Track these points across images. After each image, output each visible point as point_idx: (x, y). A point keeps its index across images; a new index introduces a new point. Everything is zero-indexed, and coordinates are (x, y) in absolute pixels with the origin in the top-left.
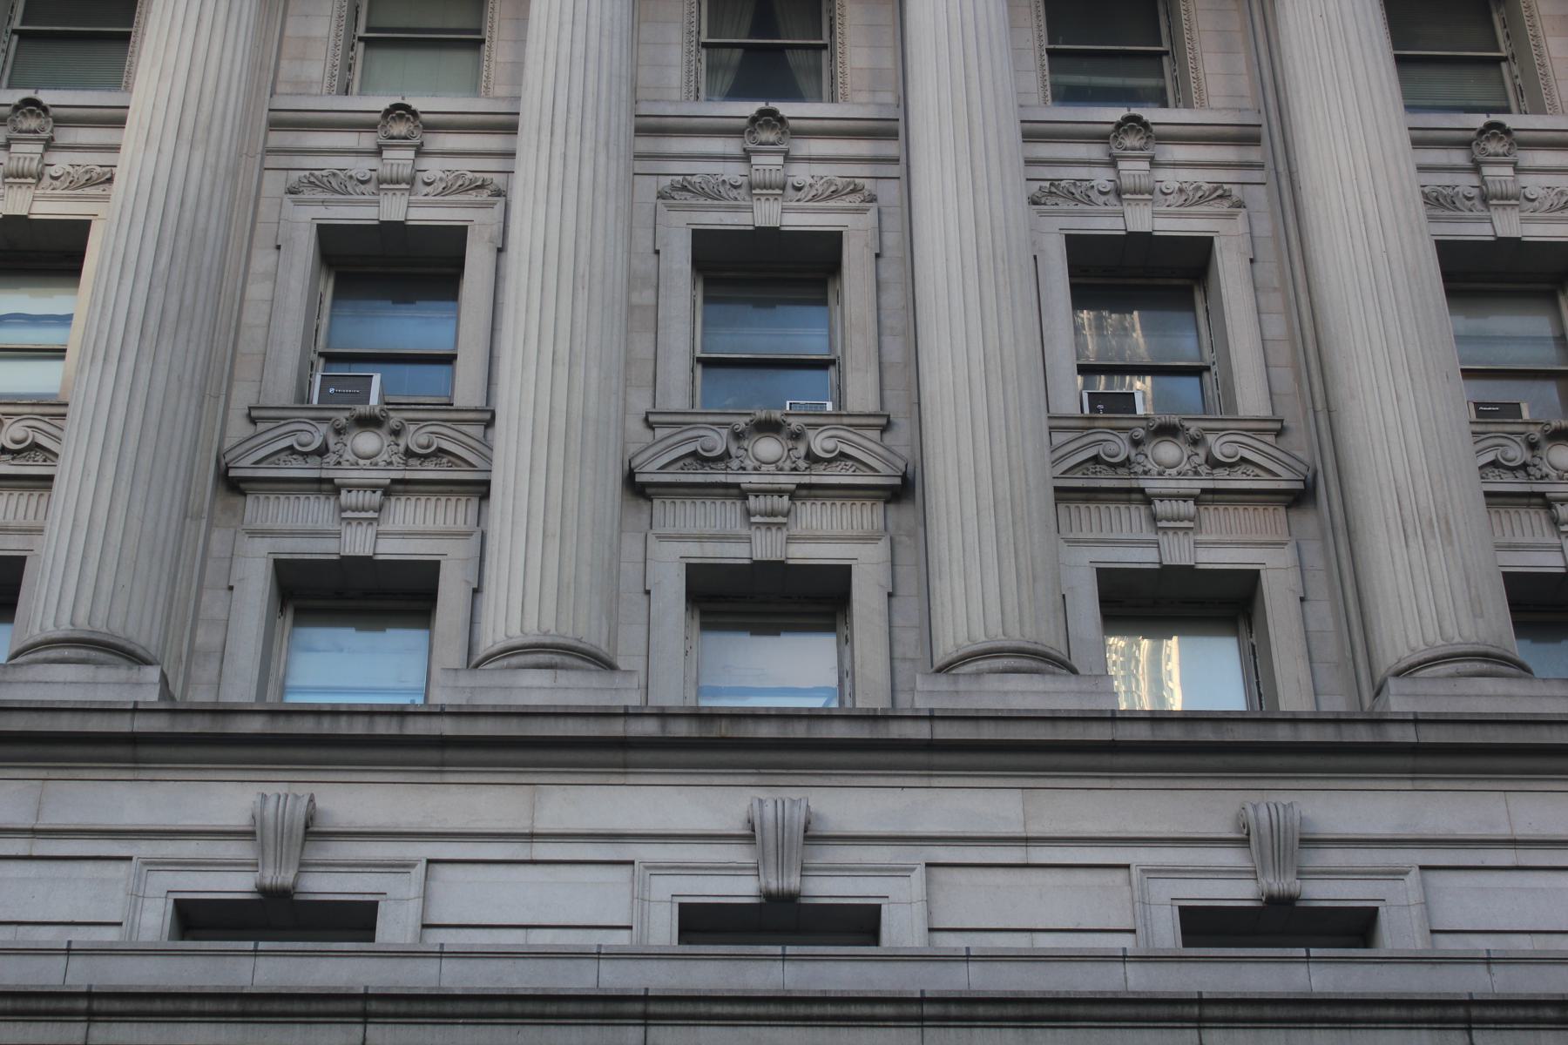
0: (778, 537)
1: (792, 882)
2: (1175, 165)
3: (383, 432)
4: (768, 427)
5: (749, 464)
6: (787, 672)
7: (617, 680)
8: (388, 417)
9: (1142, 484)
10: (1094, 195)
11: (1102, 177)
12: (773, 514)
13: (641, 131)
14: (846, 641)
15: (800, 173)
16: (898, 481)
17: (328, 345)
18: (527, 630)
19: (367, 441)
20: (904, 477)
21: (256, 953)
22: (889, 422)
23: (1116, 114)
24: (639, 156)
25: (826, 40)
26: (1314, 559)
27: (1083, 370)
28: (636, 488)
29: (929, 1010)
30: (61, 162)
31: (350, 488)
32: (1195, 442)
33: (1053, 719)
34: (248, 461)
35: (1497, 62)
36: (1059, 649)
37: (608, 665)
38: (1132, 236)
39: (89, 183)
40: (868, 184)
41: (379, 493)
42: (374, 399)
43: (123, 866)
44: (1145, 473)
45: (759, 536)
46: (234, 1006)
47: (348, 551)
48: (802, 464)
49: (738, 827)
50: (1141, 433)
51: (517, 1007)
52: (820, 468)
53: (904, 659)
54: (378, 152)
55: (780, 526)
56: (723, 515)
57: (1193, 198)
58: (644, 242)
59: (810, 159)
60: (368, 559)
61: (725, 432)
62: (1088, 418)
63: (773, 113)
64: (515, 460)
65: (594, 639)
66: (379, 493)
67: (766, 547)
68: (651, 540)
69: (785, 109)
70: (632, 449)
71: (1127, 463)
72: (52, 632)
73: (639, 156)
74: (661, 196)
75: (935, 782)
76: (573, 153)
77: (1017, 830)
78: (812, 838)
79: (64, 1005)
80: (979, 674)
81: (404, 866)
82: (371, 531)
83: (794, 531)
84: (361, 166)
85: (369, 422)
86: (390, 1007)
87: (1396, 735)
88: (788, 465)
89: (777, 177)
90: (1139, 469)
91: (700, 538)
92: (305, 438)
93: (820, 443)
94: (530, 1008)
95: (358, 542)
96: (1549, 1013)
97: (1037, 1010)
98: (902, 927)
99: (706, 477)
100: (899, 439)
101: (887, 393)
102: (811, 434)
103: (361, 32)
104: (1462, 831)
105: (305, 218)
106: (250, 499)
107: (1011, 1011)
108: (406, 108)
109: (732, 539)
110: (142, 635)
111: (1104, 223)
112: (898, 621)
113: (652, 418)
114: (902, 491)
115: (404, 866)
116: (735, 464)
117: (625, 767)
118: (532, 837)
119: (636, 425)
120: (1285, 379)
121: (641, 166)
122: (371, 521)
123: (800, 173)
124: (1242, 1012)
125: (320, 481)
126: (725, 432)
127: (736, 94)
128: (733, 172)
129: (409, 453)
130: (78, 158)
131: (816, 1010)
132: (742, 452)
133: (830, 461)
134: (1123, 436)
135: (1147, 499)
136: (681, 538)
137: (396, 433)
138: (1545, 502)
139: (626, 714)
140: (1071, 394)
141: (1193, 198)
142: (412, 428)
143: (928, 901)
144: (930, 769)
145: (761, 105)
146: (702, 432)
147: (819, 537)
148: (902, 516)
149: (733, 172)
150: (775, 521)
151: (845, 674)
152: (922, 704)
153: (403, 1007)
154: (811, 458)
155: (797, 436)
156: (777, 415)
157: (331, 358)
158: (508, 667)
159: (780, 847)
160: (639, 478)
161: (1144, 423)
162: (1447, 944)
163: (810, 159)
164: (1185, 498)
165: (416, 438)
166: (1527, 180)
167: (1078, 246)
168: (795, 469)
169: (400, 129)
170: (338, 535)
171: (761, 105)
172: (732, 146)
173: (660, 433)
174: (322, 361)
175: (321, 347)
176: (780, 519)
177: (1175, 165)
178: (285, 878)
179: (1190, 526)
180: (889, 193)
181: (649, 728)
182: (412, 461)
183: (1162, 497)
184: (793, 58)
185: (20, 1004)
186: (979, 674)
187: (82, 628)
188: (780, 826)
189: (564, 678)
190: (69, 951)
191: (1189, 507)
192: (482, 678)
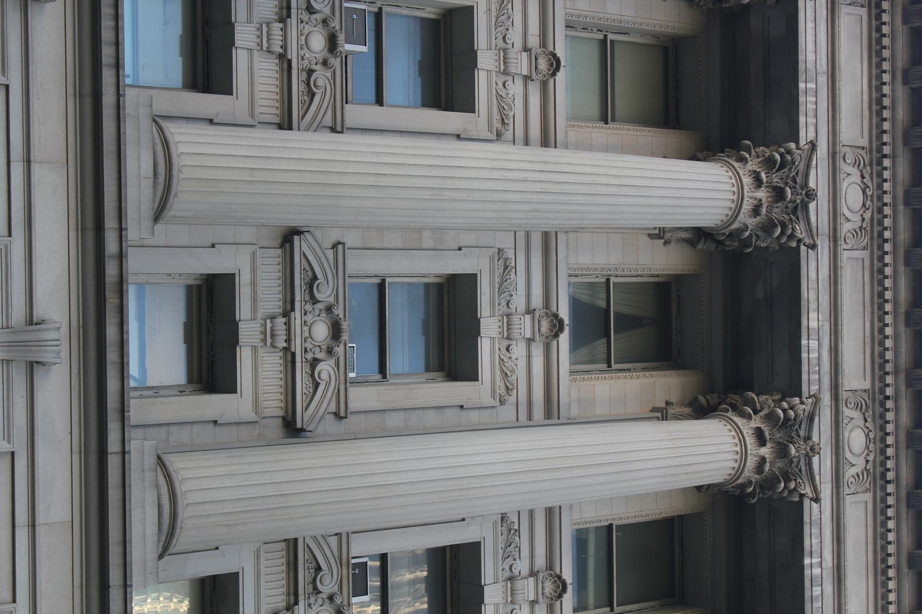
0: (256, 340)
3: (325, 54)
4: (336, 331)
5: (309, 318)
6: (156, 349)
7: (147, 223)
8: (336, 57)
9: (301, 603)
10: (510, 561)
11: (522, 566)
12: (273, 336)
13: (546, 236)
14: (181, 391)
15: (519, 350)
16: (299, 425)
17: (387, 14)
18: (183, 157)
19: (318, 42)
20: (302, 430)
22: (342, 418)
23: (568, 575)
24: (528, 235)
25: (614, 366)
28: (289, 237)
31: (284, 30)
33: (125, 542)
36: (176, 546)
37: (157, 216)
38: (481, 589)
40: (512, 399)
41: (281, 51)
42: (349, 47)
44: (310, 605)
45: (257, 326)
47: (238, 29)
48: (310, 356)
49: (38, 313)
50: (338, 601)
52: (307, 368)
53: (168, 433)
54: (526, 49)
55: (264, 341)
56: (271, 301)
58: (467, 239)
59: (529, 357)
60: (233, 43)
61: (332, 300)
62: (348, 563)
63: (561, 329)
64: (307, 147)
65: (179, 205)
66: (281, 51)
67: (249, 331)
68: (249, 249)
69: (564, 338)
70: (318, 233)
71: (316, 591)
73: (528, 235)
74: (500, 251)
75: (76, 457)
76: (529, 187)
77: (40, 518)
78: (32, 366)
80: (157, 486)
82: (253, 45)
83: (261, 351)
84: (515, 37)
85: (332, 43)
88: (308, 345)
89: (516, 333)
90: (312, 600)
91: (254, 283)
93: (325, 369)
99: (298, 286)
100: (330, 424)
101: (363, 416)
102: (332, 362)
103: (610, 37)
108: (558, 68)
109: (254, 307)
111: (489, 569)
112: (196, 428)
113: (340, 247)
114: (292, 429)
116: (308, 307)
118: (28, 161)
119: (334, 235)
121: (521, 236)
122: (260, 45)
123: (519, 350)
125: (289, 8)
126: (332, 300)
127: (576, 305)
128: (519, 302)
129: (310, 72)
132: (317, 312)
133: (312, 375)
134: (336, 588)
136: (254, 270)
137: (325, 63)
139: (121, 230)
140: (364, 549)
142: (329, 75)
145: (567, 321)
146: (331, 283)
147: (257, 368)
148: (275, 428)
149: (519, 302)
150: (268, 337)
151: (157, 391)
152: (134, 446)
154: (315, 362)
155: (330, 352)
156: (345, 337)
157: (378, 16)
158: (154, 144)
159: (24, 343)
160: (296, 238)
161: (345, 603)
163: (529, 357)
165: (321, 77)
167: (473, 549)
168: (306, 351)
169: (543, 64)
170: (250, 21)
171: (567, 321)
172: (537, 301)
173: (330, 253)
174: (376, 10)
175: (385, 9)
176: (269, 341)
180: (507, 414)
181: (111, 247)
182: (305, 74)
184: (601, 343)
186: (157, 486)
188: (40, 344)
189: (147, 184)
192: (146, 125)
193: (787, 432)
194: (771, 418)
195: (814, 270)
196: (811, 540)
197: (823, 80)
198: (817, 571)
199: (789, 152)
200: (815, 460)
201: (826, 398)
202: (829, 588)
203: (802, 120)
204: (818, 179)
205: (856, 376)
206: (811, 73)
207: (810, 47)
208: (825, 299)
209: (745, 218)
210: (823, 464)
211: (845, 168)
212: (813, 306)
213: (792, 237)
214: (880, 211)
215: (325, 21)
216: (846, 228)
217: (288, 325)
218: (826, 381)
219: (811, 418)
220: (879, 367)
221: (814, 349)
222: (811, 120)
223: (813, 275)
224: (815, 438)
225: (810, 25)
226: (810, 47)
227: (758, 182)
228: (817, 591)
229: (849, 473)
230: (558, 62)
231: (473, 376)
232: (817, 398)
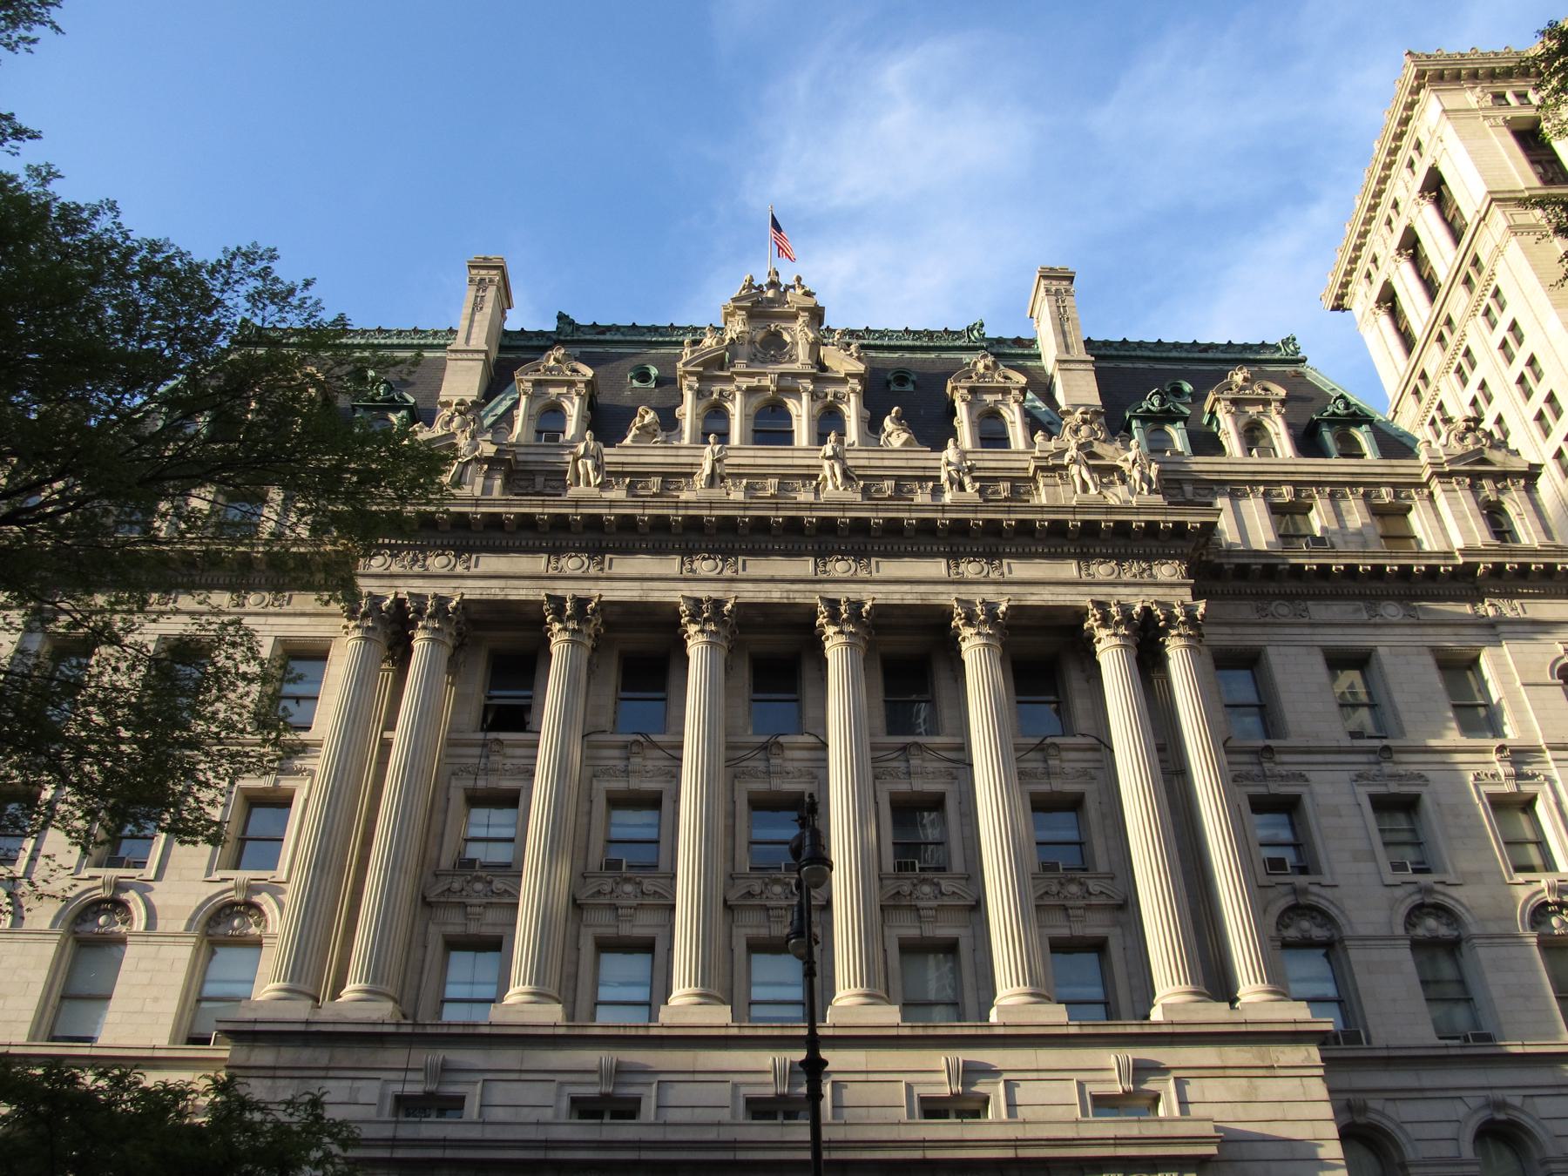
138: (1065, 908)
166: (1065, 765)
178: (610, 1089)
196: (895, 599)
202: (923, 588)
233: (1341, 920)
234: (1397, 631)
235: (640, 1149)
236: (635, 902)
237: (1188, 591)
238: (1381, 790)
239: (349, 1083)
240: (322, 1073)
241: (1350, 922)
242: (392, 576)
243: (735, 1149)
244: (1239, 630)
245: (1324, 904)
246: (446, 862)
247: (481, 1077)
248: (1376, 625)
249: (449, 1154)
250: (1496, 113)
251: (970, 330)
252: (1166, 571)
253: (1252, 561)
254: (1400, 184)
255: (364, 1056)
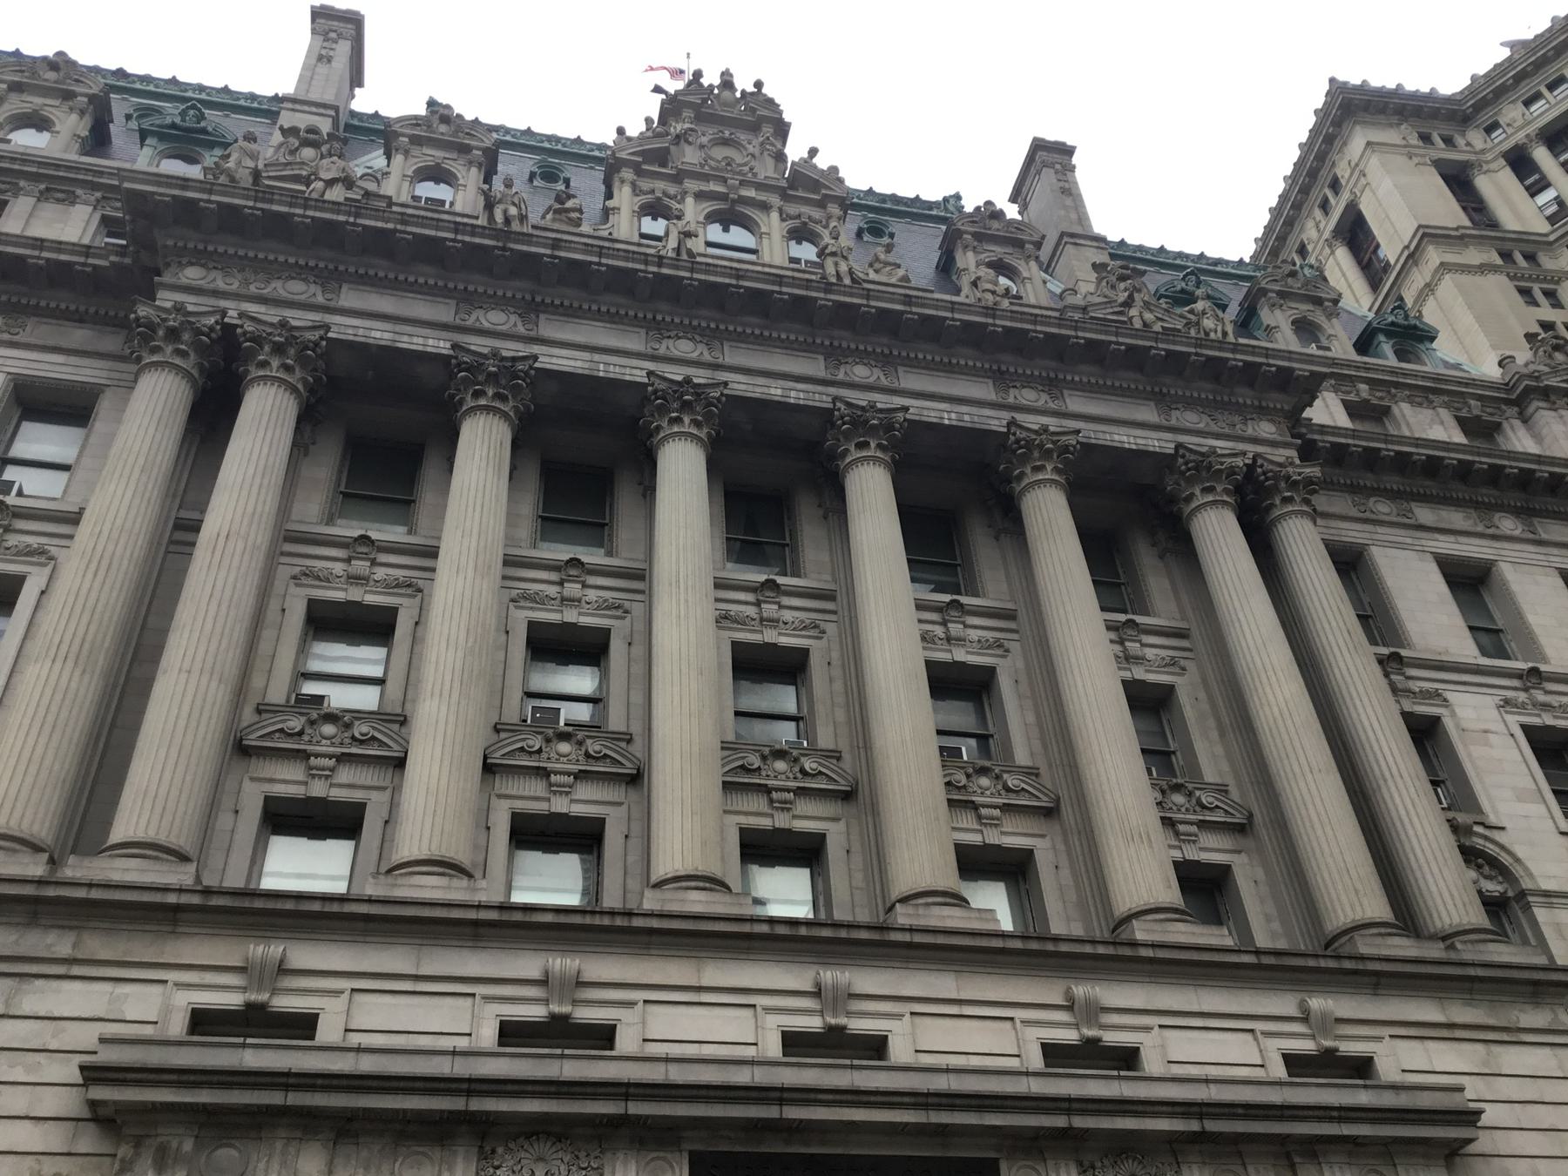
1: (842, 1021)
2: (975, 627)
15: (788, 615)
19: (564, 747)
21: (562, 1056)
26: (1061, 847)
27: (939, 732)
29: (930, 1100)
30: (380, 573)
32: (998, 777)
34: (498, 755)
35: (1119, 585)
39: (397, 586)
40: (822, 624)
43: (469, 1000)
46: (553, 1089)
51: (712, 1093)
52: (809, 779)
55: (788, 810)
57: (984, 645)
63: (774, 581)
67: (782, 821)
72: (416, 854)
79: (454, 1086)
80: (928, 905)
81: (630, 1004)
85: (564, 737)
86: (641, 1091)
87: (1144, 952)
92: (531, 743)
93: (809, 765)
94: (718, 1093)
95: (560, 805)
96: (1240, 1111)
97: (987, 1102)
98: (899, 1051)
102: (803, 759)
104: (1176, 1007)
105: (521, 618)
106: (498, 777)
107: (974, 1102)
108: (578, 560)
110: (463, 856)
111: (941, 656)
115: (630, 1004)
117: (748, 950)
118: (700, 989)
120: (1037, 744)
122: (567, 793)
124: (1090, 1106)
125: (538, 768)
129: (588, 755)
130: (390, 571)
131: (872, 1099)
133: (813, 776)
135: (974, 807)
137: (580, 743)
141: (984, 645)
143: (913, 1034)
144: (907, 959)
150: (785, 807)
153: (648, 1091)
154: (803, 772)
159: (835, 999)
162: (1177, 1070)
164: (995, 807)
165: (593, 747)
169: (573, 572)
177: (975, 627)
179: (994, 823)
181: (765, 928)
183: (984, 806)
185: (428, 1085)
186: (928, 905)
187: (436, 852)
190: (454, 1053)
191: (997, 812)
193: (862, 424)
194: (848, 436)
195: (741, 385)
197: (597, 357)
198: (953, 416)
199: (655, 392)
200: (879, 405)
201: (832, 390)
202: (964, 409)
203: (627, 378)
204: (676, 373)
205: (815, 366)
206: (593, 366)
207: (572, 363)
208: (761, 381)
209: (703, 434)
210: (883, 401)
211: (662, 351)
212: (766, 390)
213: (718, 400)
214: (695, 328)
215: (548, 741)
216: (707, 357)
217: (778, 790)
218: (820, 388)
219: (849, 405)
220: (808, 348)
221: (797, 395)
222: (628, 371)
223: (743, 387)
224: (864, 404)
225: (554, 360)
226: (572, 363)
227: (678, 420)
228: (967, 418)
229: (884, 382)
230: (572, 560)
231: (805, 653)
232: (835, 399)
233: (1517, 871)
234: (1518, 546)
235: (627, 1097)
236: (575, 768)
237: (1293, 453)
238: (1535, 721)
239: (106, 987)
240: (61, 970)
241: (1531, 875)
242: (216, 293)
243: (781, 1102)
244: (1334, 523)
245: (1491, 849)
246: (278, 694)
247: (346, 984)
248: (1494, 537)
249: (295, 1099)
250: (1422, 151)
251: (946, 200)
252: (1266, 429)
253: (1350, 441)
254: (1310, 224)
255: (140, 948)
